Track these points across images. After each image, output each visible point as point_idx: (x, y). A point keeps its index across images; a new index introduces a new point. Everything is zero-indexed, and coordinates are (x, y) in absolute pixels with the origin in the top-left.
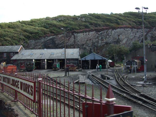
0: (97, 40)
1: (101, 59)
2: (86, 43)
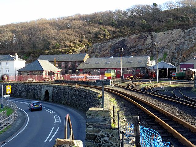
0: (183, 40)
1: (171, 67)
2: (167, 45)
